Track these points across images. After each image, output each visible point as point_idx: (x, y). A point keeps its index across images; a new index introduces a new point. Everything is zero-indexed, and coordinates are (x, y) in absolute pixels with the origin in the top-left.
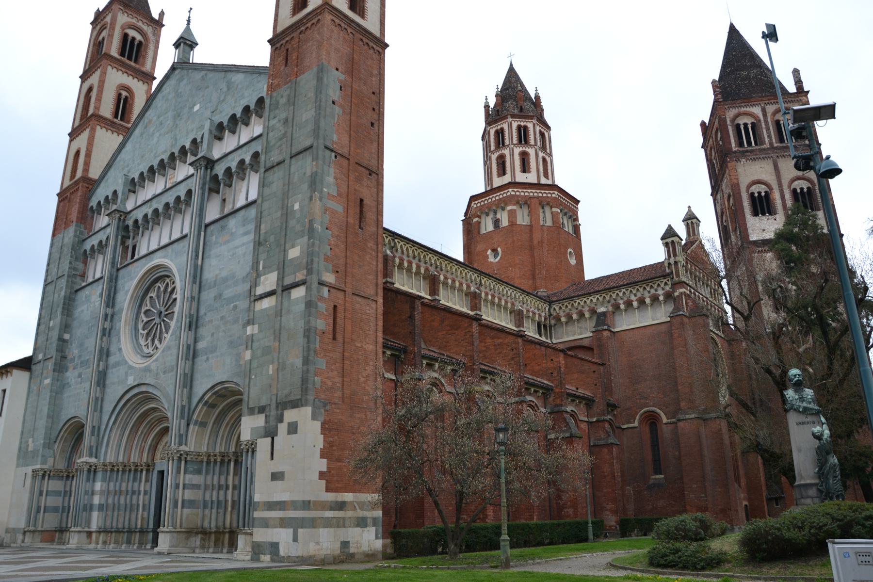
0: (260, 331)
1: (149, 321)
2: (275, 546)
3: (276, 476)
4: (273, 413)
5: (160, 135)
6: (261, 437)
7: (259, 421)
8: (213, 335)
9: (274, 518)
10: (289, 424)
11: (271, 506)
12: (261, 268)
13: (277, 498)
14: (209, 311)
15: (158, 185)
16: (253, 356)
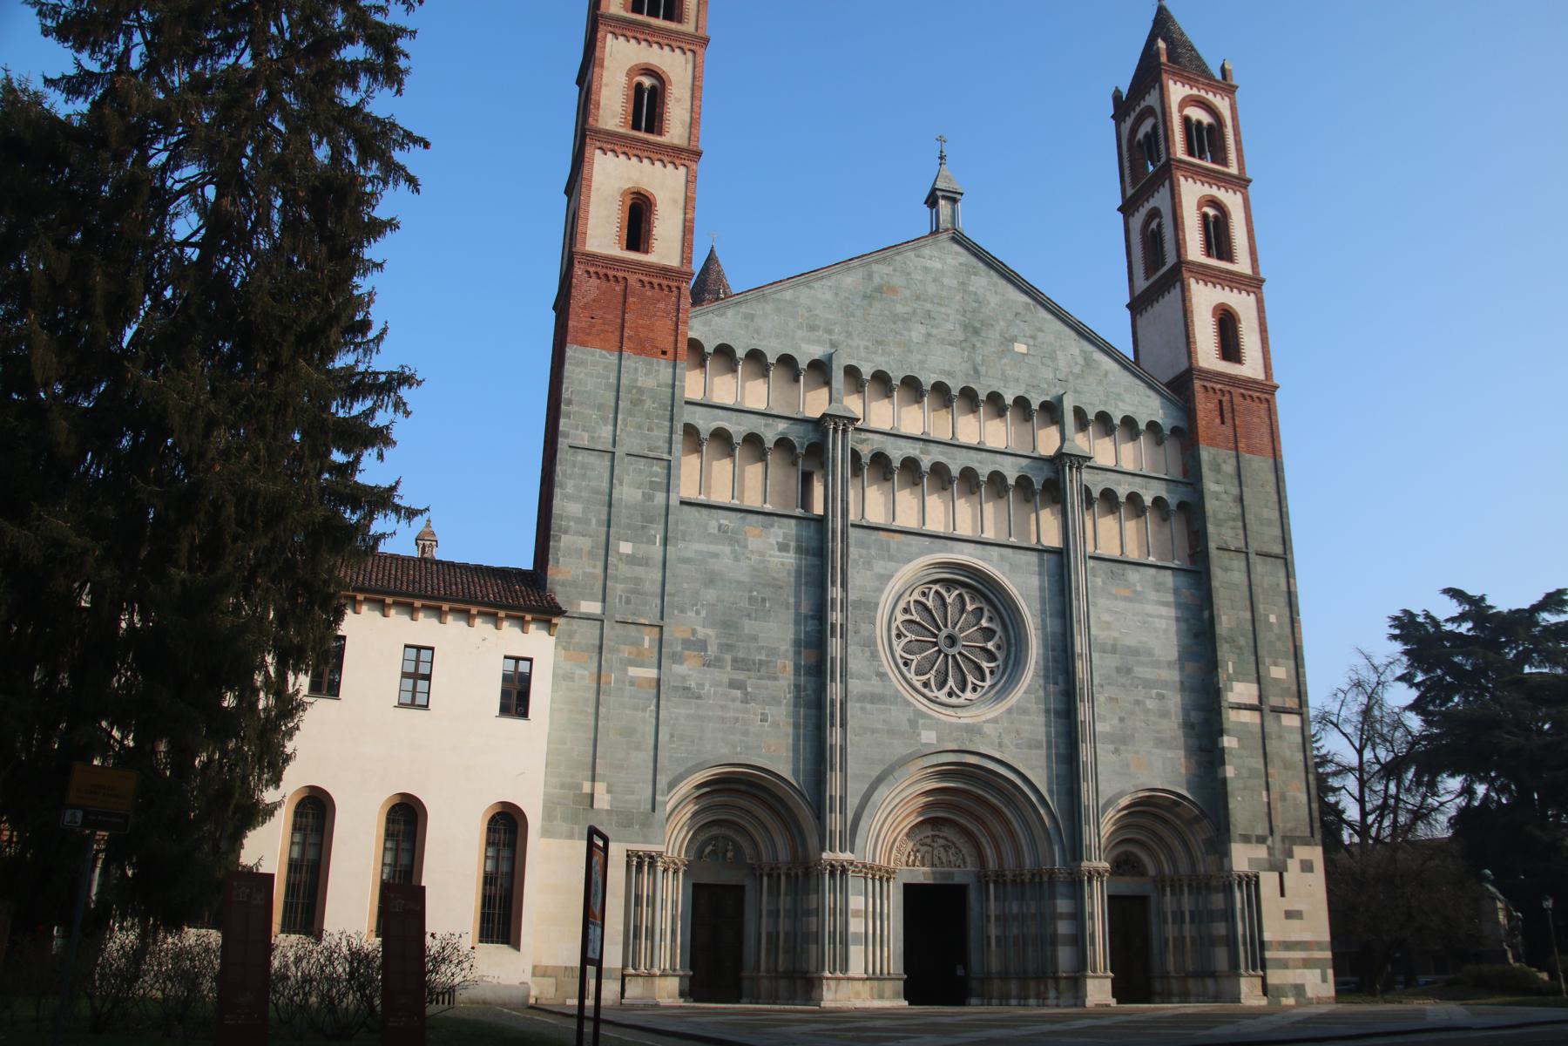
0: (1242, 746)
1: (917, 640)
2: (1299, 989)
3: (1290, 915)
4: (1278, 845)
5: (929, 335)
6: (1265, 870)
7: (1261, 852)
8: (1122, 720)
9: (1294, 959)
10: (1302, 862)
11: (1288, 946)
12: (1231, 671)
13: (1294, 937)
14: (1109, 684)
15: (915, 419)
16: (1237, 776)
